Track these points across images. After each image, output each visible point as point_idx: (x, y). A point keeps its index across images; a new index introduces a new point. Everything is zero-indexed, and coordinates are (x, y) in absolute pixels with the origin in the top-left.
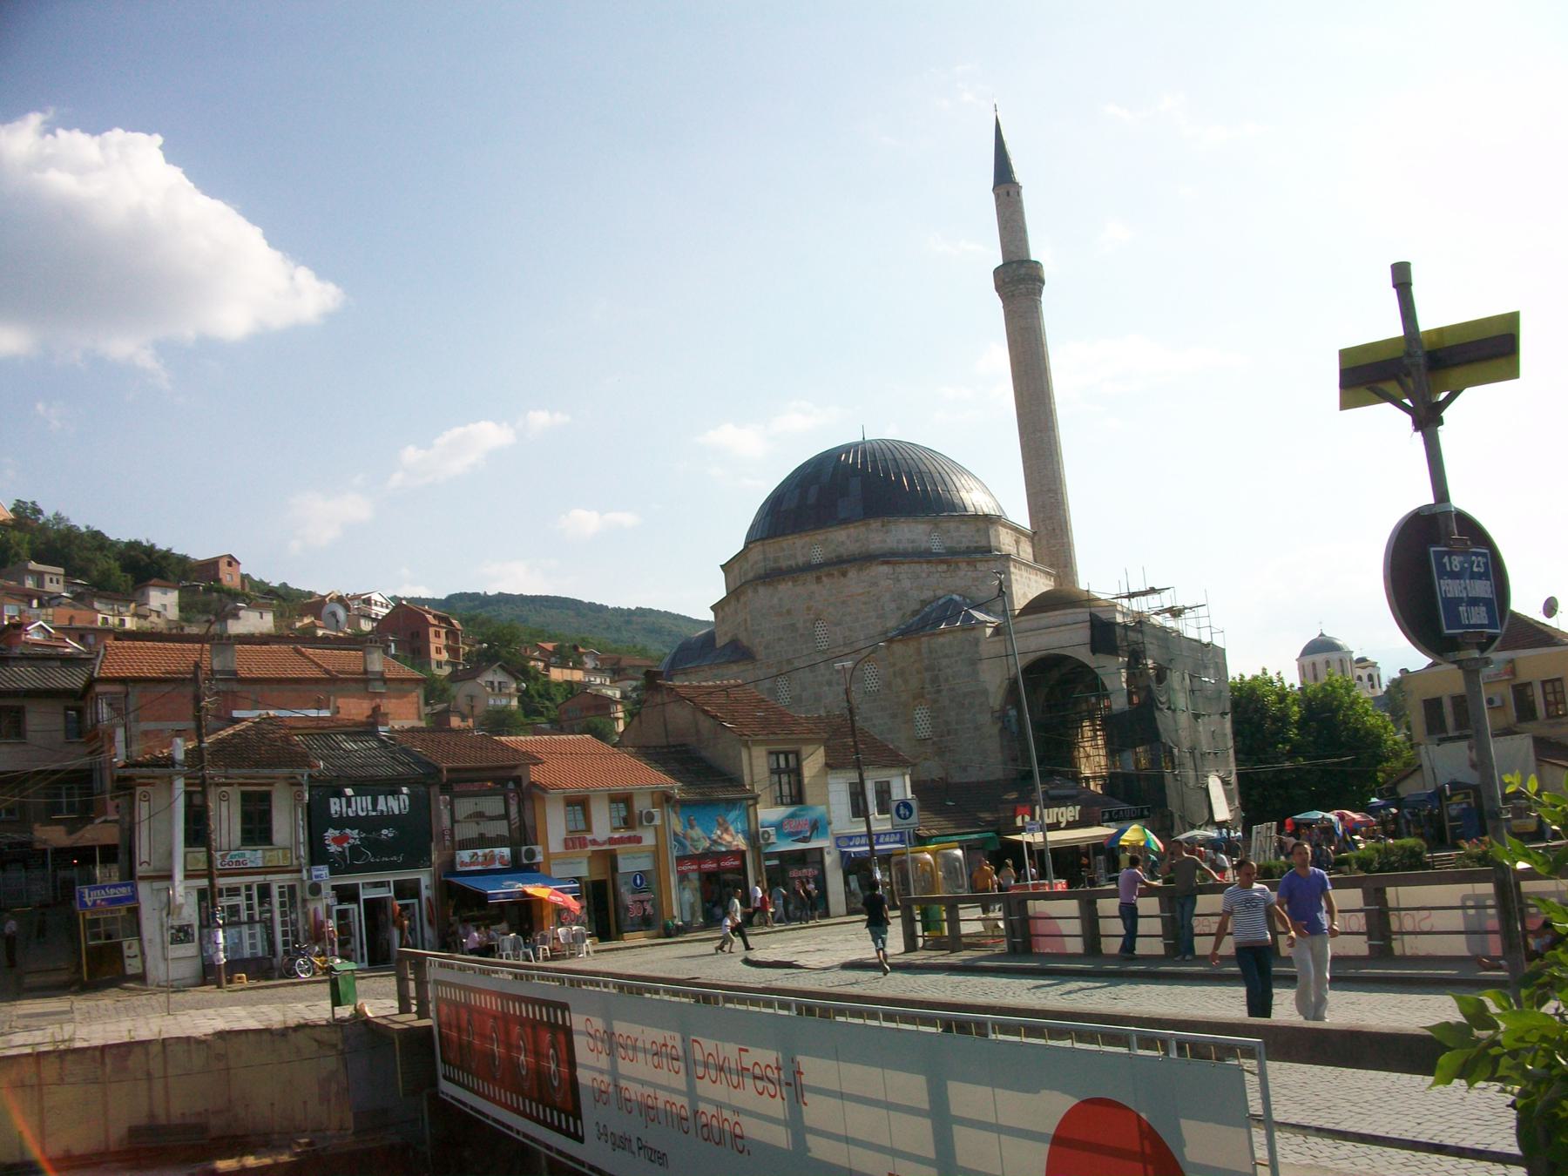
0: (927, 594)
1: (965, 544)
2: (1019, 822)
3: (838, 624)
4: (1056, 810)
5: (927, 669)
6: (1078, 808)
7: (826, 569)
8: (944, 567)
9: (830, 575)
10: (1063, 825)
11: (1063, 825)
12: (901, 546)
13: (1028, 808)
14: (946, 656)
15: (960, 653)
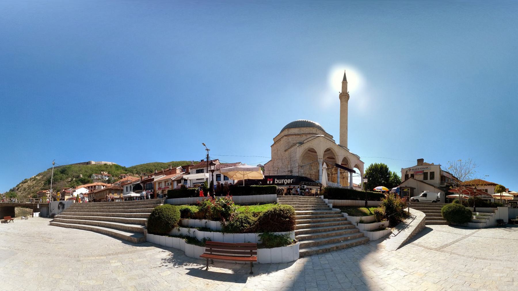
0: (295, 142)
1: (307, 132)
2: (268, 182)
3: (280, 150)
4: (283, 180)
5: (290, 156)
6: (292, 180)
7: (278, 141)
8: (299, 136)
9: (279, 141)
10: (285, 184)
11: (285, 184)
12: (292, 134)
13: (272, 179)
14: (292, 153)
15: (294, 152)
